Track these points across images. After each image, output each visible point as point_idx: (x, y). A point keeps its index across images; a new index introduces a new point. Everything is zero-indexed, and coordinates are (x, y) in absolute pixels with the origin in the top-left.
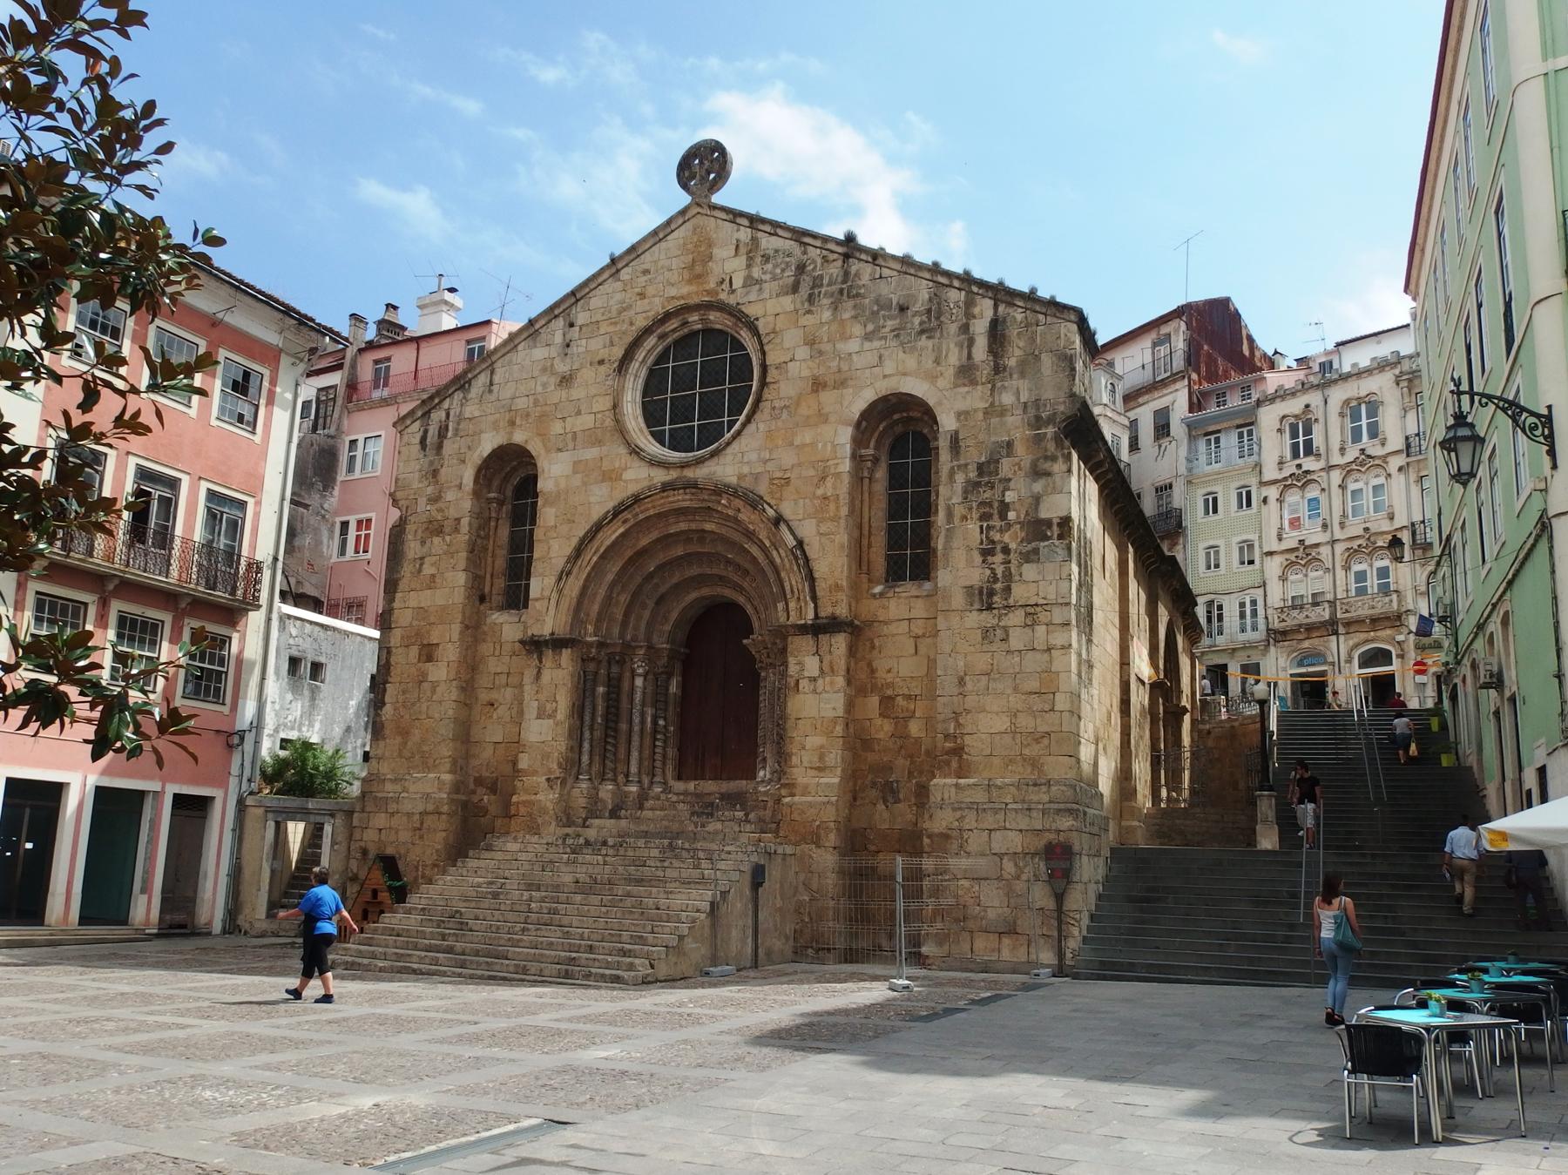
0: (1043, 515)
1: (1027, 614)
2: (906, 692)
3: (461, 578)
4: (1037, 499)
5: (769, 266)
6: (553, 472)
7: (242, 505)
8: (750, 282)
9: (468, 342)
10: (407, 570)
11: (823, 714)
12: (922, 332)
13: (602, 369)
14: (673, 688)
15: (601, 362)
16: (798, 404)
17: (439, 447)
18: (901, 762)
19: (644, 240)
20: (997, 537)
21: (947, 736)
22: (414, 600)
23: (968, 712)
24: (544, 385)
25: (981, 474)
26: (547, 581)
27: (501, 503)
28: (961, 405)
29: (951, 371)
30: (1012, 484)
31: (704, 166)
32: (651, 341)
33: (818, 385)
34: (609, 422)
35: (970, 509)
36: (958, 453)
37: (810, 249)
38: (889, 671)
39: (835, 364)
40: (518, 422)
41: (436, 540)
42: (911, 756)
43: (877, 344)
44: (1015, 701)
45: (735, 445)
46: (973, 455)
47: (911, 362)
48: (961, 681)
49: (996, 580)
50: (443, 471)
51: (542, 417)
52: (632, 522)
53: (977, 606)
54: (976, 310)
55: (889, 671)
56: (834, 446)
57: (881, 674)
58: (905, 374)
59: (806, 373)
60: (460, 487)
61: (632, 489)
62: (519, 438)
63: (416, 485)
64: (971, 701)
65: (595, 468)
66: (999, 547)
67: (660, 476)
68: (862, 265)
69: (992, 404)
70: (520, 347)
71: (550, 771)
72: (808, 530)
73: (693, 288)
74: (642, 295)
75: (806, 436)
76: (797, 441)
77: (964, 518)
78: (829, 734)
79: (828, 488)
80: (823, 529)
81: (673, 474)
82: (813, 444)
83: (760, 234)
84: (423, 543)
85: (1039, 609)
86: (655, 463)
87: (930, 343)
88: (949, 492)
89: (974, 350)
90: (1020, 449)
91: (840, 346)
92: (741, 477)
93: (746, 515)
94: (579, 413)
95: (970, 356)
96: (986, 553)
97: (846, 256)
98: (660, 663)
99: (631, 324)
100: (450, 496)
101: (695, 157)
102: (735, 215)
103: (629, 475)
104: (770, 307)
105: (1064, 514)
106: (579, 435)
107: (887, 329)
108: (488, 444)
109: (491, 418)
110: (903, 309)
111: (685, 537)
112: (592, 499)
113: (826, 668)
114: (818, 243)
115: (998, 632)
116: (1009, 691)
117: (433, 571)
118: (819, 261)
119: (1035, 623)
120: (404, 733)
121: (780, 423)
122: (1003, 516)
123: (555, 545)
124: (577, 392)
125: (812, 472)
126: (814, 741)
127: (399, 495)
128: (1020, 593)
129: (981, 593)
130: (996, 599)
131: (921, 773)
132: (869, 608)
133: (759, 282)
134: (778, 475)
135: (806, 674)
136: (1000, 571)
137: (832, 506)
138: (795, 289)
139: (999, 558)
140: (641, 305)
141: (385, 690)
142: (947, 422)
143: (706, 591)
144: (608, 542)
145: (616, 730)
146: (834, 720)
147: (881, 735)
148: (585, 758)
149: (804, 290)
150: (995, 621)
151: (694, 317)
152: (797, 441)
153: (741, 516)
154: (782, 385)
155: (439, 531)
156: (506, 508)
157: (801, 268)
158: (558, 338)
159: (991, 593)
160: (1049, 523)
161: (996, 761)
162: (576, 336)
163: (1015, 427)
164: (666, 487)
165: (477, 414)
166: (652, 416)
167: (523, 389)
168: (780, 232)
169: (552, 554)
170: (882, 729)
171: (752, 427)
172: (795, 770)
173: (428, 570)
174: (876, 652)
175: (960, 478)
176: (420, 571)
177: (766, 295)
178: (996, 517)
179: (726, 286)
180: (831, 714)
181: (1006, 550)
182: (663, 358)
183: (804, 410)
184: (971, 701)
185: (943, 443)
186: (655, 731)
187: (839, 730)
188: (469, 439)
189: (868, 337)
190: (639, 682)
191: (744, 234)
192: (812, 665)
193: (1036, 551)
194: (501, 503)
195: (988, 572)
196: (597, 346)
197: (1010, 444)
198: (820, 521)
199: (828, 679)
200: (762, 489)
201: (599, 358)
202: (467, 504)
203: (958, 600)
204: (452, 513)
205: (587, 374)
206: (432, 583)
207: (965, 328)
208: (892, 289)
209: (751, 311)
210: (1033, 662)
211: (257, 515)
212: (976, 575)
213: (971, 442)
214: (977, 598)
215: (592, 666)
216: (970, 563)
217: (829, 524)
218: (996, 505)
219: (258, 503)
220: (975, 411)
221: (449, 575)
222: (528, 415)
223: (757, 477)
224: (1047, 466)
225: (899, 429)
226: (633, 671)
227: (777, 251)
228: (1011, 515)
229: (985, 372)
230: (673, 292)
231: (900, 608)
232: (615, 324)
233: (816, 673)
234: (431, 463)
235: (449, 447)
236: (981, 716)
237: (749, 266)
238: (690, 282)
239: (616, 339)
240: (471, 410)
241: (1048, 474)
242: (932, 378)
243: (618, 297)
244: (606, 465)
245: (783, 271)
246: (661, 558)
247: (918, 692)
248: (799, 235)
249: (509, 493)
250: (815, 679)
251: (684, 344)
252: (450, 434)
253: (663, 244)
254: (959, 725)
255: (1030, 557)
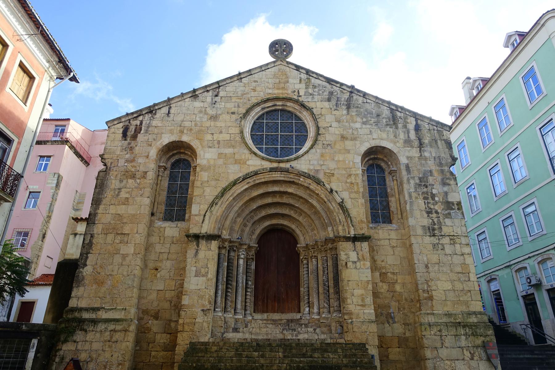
0: (450, 200)
1: (451, 239)
2: (392, 271)
3: (147, 201)
4: (446, 194)
5: (316, 90)
6: (205, 156)
7: (9, 141)
8: (307, 94)
9: (56, 126)
10: (108, 195)
11: (361, 279)
12: (387, 125)
13: (233, 116)
14: (253, 267)
15: (233, 113)
16: (335, 144)
17: (134, 137)
18: (394, 304)
19: (256, 68)
20: (432, 207)
21: (424, 291)
22: (113, 210)
23: (432, 280)
24: (200, 117)
25: (421, 181)
26: (202, 206)
27: (165, 169)
28: (407, 154)
29: (402, 141)
30: (435, 187)
31: (280, 49)
32: (258, 109)
33: (343, 138)
34: (238, 138)
35: (419, 194)
36: (410, 172)
37: (334, 87)
38: (383, 261)
39: (350, 131)
40: (185, 131)
41: (130, 181)
42: (398, 301)
43: (368, 126)
44: (454, 276)
45: (306, 156)
46: (416, 174)
47: (384, 135)
48: (427, 267)
49: (435, 224)
50: (137, 148)
51: (200, 131)
52: (252, 184)
53: (428, 234)
54: (409, 121)
55: (383, 261)
56: (354, 163)
57: (379, 262)
58: (382, 139)
59: (337, 132)
60: (147, 157)
61: (252, 169)
62: (185, 138)
63: (118, 152)
64: (432, 275)
65: (226, 160)
66: (433, 211)
67: (268, 165)
68: (358, 97)
69: (421, 155)
70: (186, 100)
71: (203, 305)
72: (345, 195)
73: (280, 91)
74: (254, 90)
75: (340, 157)
76: (336, 159)
77: (416, 198)
78: (365, 289)
79: (353, 179)
80: (353, 195)
81: (275, 165)
82: (344, 161)
83: (311, 77)
84: (121, 181)
85: (455, 237)
86: (263, 159)
87: (391, 130)
88: (409, 187)
89: (410, 135)
90: (435, 174)
91: (352, 124)
92: (309, 169)
93: (313, 186)
94: (221, 132)
95: (409, 137)
96: (429, 213)
97: (351, 92)
98: (251, 254)
99: (249, 100)
100: (140, 160)
101: (277, 44)
102: (298, 68)
103: (250, 162)
104: (318, 105)
105: (458, 200)
106: (221, 142)
107: (372, 122)
108: (166, 139)
109: (169, 128)
110: (378, 116)
111: (274, 193)
112: (229, 171)
113: (361, 258)
114: (338, 85)
115: (440, 246)
116: (449, 272)
117: (127, 196)
118: (339, 92)
119: (454, 244)
120: (100, 283)
121: (327, 150)
122: (433, 199)
123: (208, 190)
124: (219, 124)
125: (344, 172)
126: (358, 292)
127: (106, 156)
128: (445, 230)
129: (429, 229)
130: (436, 232)
131: (404, 308)
132: (371, 233)
133: (311, 94)
134: (329, 171)
135: (351, 260)
136: (436, 220)
137: (356, 187)
138: (329, 100)
139: (434, 215)
140: (253, 94)
141: (87, 258)
142: (403, 160)
143: (274, 221)
144: (239, 191)
145: (231, 285)
146: (368, 282)
147: (382, 291)
148: (219, 299)
149: (334, 102)
150: (437, 241)
151: (280, 103)
152: (336, 159)
153: (311, 187)
154: (327, 135)
155: (133, 177)
156: (167, 172)
157: (331, 93)
158: (209, 99)
159: (434, 230)
160: (453, 204)
161: (449, 303)
162: (219, 100)
163: (431, 165)
164: (272, 170)
165: (159, 125)
166: (257, 140)
167: (188, 118)
168: (320, 78)
169: (205, 194)
170: (383, 288)
171: (313, 151)
172: (350, 306)
173: (123, 195)
174: (375, 252)
175: (412, 182)
176: (118, 195)
177: (316, 100)
178: (430, 199)
179: (296, 93)
180: (366, 279)
181: (437, 212)
182: (261, 117)
183: (338, 146)
184: (432, 275)
185: (403, 168)
186: (246, 288)
187: (370, 287)
188: (154, 136)
189: (364, 123)
190: (241, 262)
191: (304, 76)
192: (353, 256)
193: (449, 214)
194: (165, 169)
195: (431, 221)
196: (230, 106)
197: (431, 171)
198: (350, 193)
199: (362, 262)
200: (321, 176)
201: (232, 111)
202: (152, 166)
203: (420, 231)
204: (142, 169)
205: (226, 117)
206: (126, 202)
207: (405, 126)
208: (371, 106)
209: (311, 105)
210: (457, 260)
211: (17, 149)
212: (426, 222)
213: (415, 169)
214: (428, 231)
215: (223, 251)
216: (422, 216)
217: (354, 194)
218: (430, 194)
219: (19, 143)
220: (415, 157)
221: (138, 199)
222: (191, 130)
223: (317, 171)
224: (448, 181)
225: (371, 162)
226: (238, 256)
227: (319, 85)
228: (437, 199)
229: (416, 143)
230: (270, 91)
231: (385, 234)
232: (241, 99)
233: (356, 260)
234: (129, 144)
235: (140, 137)
236: (439, 282)
237: (306, 88)
238: (278, 89)
239: (241, 105)
240: (154, 123)
241: (449, 185)
242: (395, 143)
243: (242, 88)
244: (237, 157)
245: (323, 92)
246: (260, 203)
247: (397, 271)
248: (329, 81)
249: (169, 165)
250: (355, 262)
251: (271, 113)
252: (142, 132)
253: (263, 72)
254: (429, 286)
255: (448, 216)
